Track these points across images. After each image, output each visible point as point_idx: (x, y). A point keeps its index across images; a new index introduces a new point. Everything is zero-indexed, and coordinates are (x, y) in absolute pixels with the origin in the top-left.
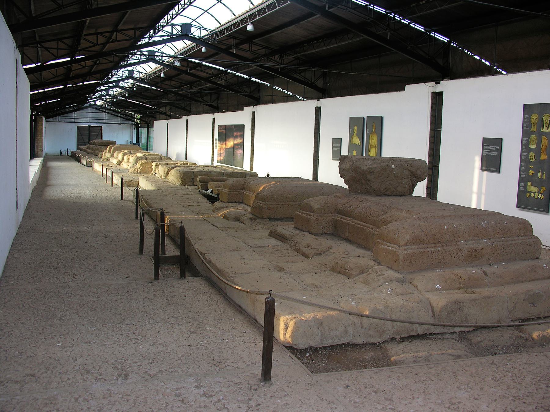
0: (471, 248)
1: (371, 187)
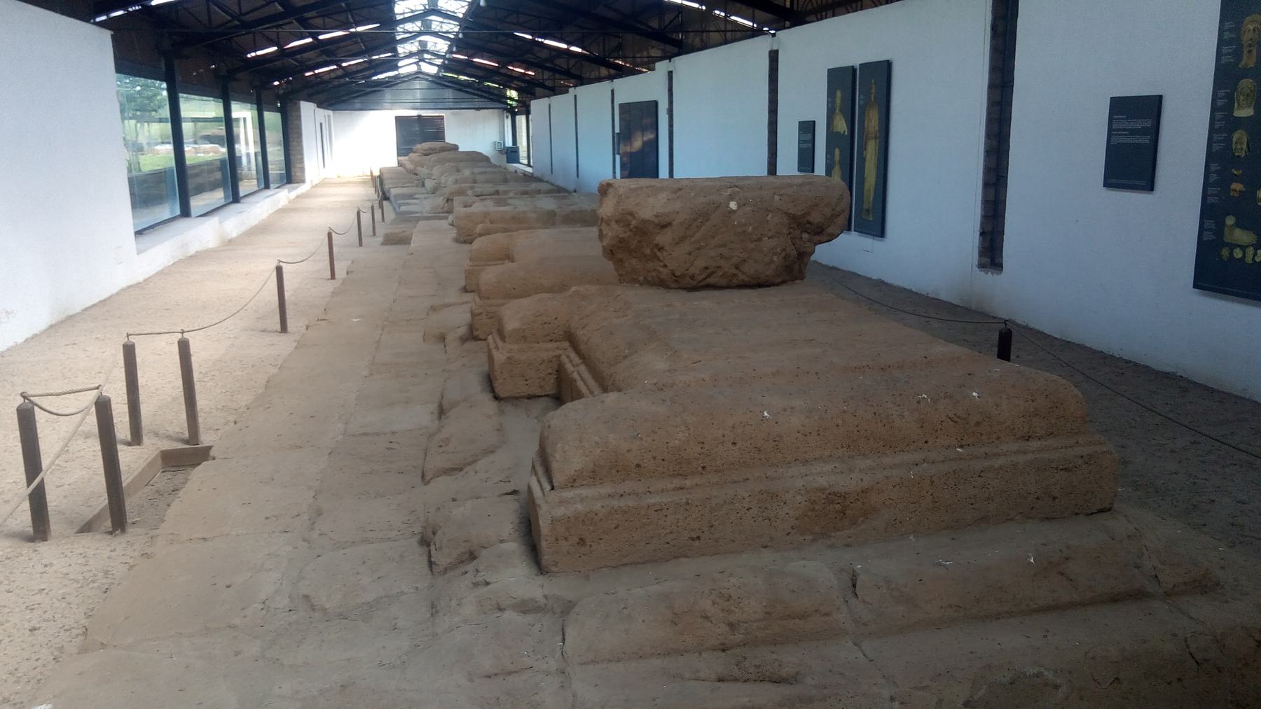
0: (822, 490)
1: (665, 266)
